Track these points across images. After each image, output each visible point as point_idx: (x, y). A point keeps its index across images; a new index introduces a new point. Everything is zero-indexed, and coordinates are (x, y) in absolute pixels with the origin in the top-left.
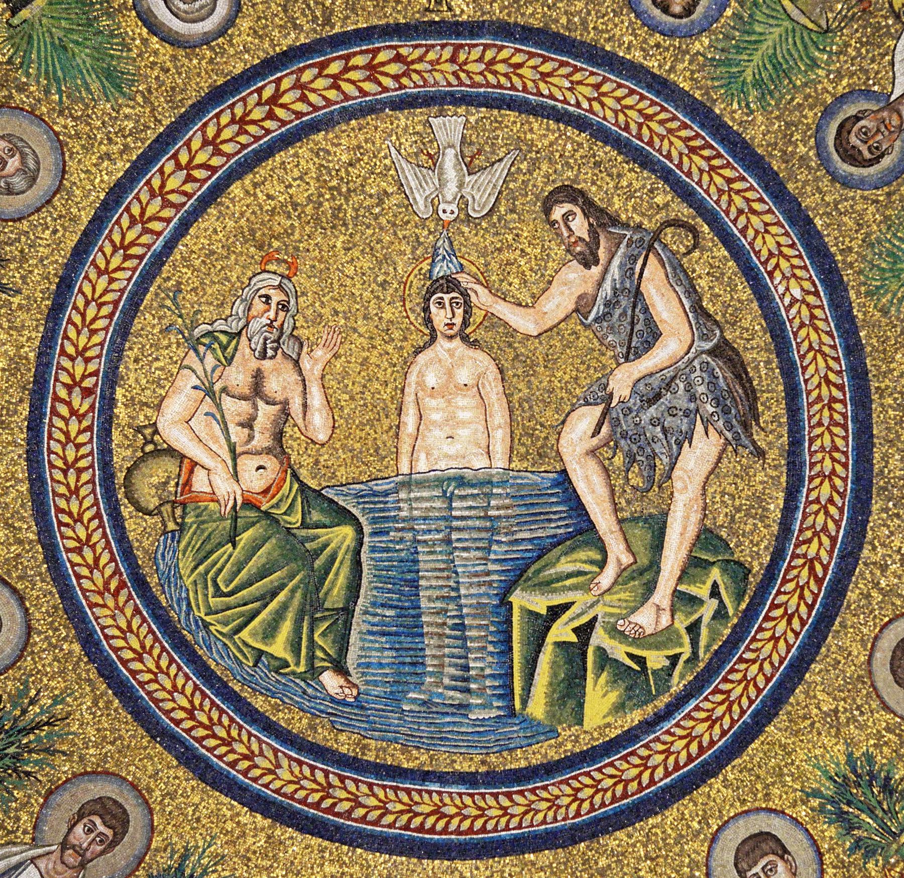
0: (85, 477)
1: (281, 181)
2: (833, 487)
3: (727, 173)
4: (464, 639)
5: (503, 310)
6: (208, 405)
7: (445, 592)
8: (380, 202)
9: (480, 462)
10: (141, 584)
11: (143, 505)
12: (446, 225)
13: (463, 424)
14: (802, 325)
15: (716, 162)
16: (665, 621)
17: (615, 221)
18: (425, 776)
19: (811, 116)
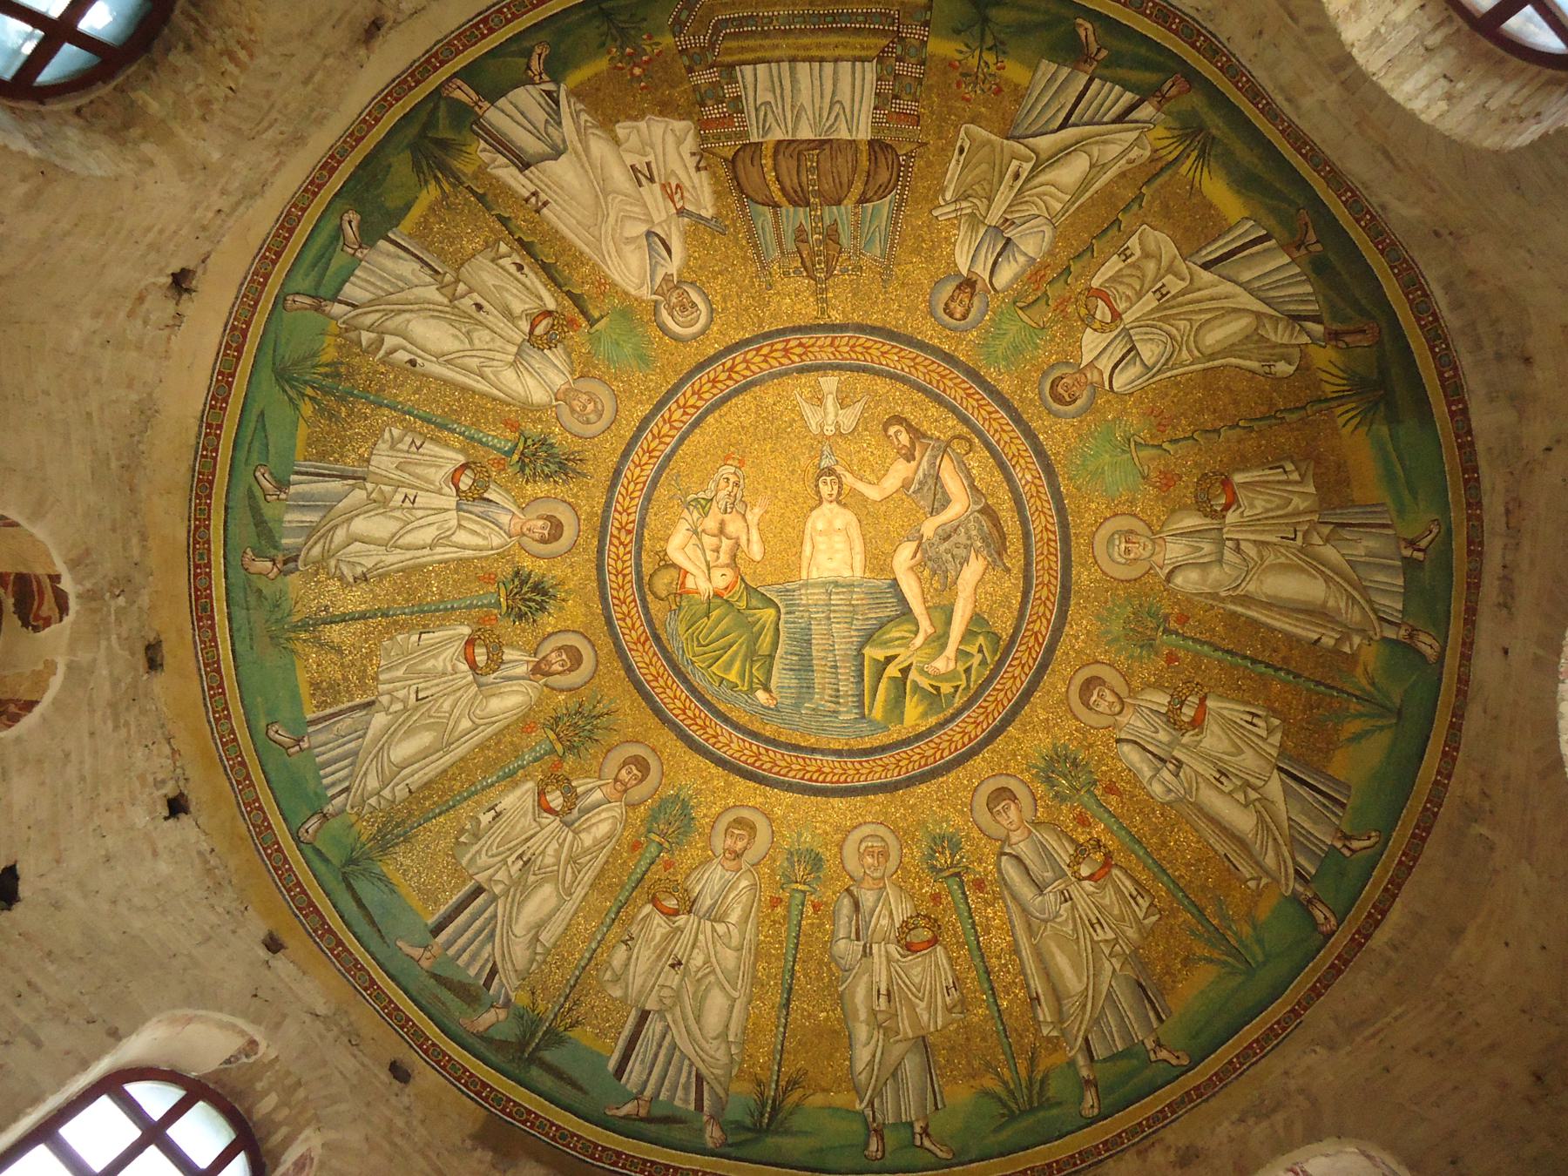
0: (628, 578)
1: (735, 413)
2: (1050, 591)
3: (988, 408)
4: (837, 674)
5: (861, 487)
6: (694, 540)
7: (826, 647)
8: (791, 425)
9: (847, 573)
10: (657, 638)
11: (659, 593)
12: (828, 438)
13: (837, 551)
14: (1032, 496)
15: (982, 402)
16: (952, 666)
17: (924, 436)
18: (813, 751)
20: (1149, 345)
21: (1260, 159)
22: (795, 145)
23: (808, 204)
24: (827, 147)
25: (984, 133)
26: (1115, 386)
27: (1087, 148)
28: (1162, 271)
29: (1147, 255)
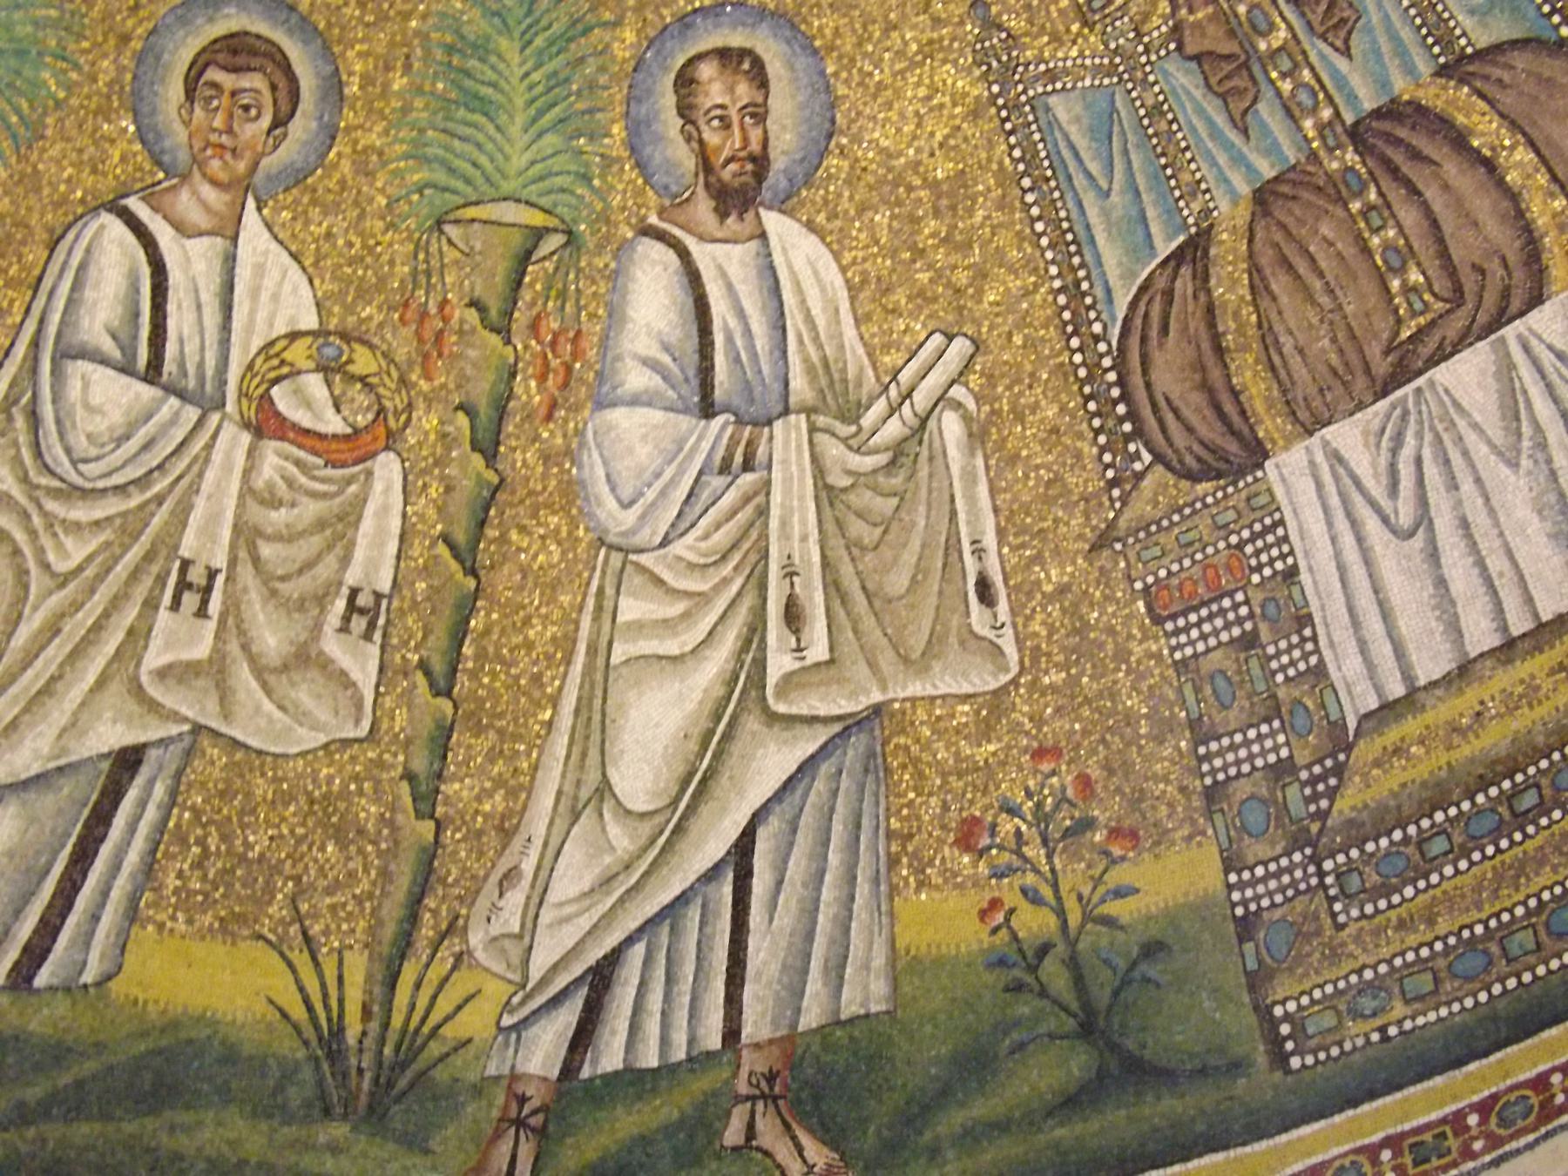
19: (356, 65)
20: (117, 417)
21: (178, 1157)
22: (1482, 318)
23: (1356, 135)
24: (1382, 367)
25: (946, 684)
26: (115, 228)
27: (646, 829)
28: (233, 647)
29: (305, 658)
